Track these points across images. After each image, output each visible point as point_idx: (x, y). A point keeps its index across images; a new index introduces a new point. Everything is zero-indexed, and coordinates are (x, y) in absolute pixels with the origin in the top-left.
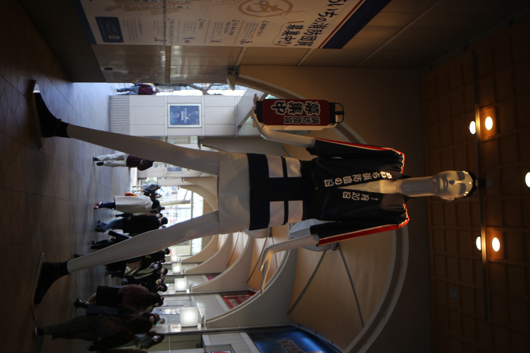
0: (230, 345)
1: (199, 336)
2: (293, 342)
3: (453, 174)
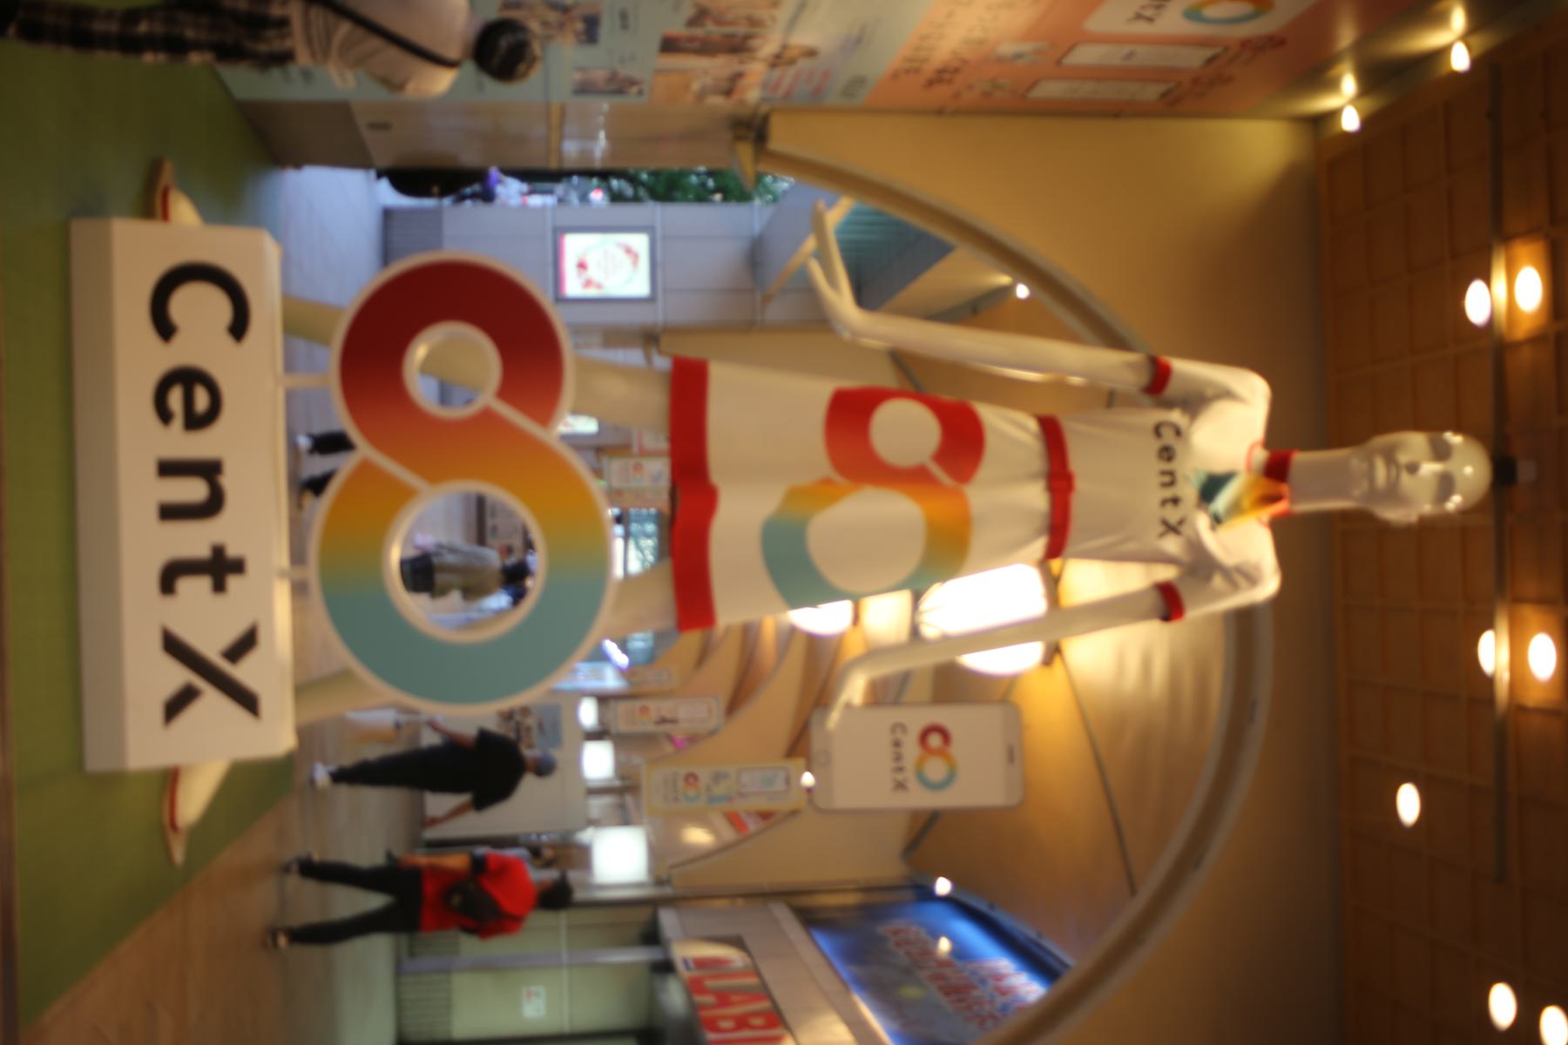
3: (1415, 443)
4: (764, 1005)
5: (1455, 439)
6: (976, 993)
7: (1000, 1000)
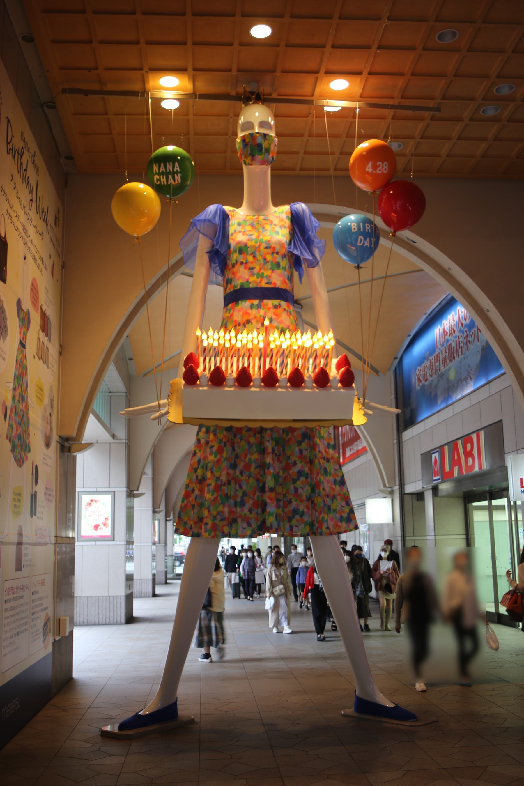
0: (421, 455)
1: (406, 496)
2: (419, 368)
4: (460, 443)
5: (242, 120)
6: (453, 345)
7: (457, 333)
